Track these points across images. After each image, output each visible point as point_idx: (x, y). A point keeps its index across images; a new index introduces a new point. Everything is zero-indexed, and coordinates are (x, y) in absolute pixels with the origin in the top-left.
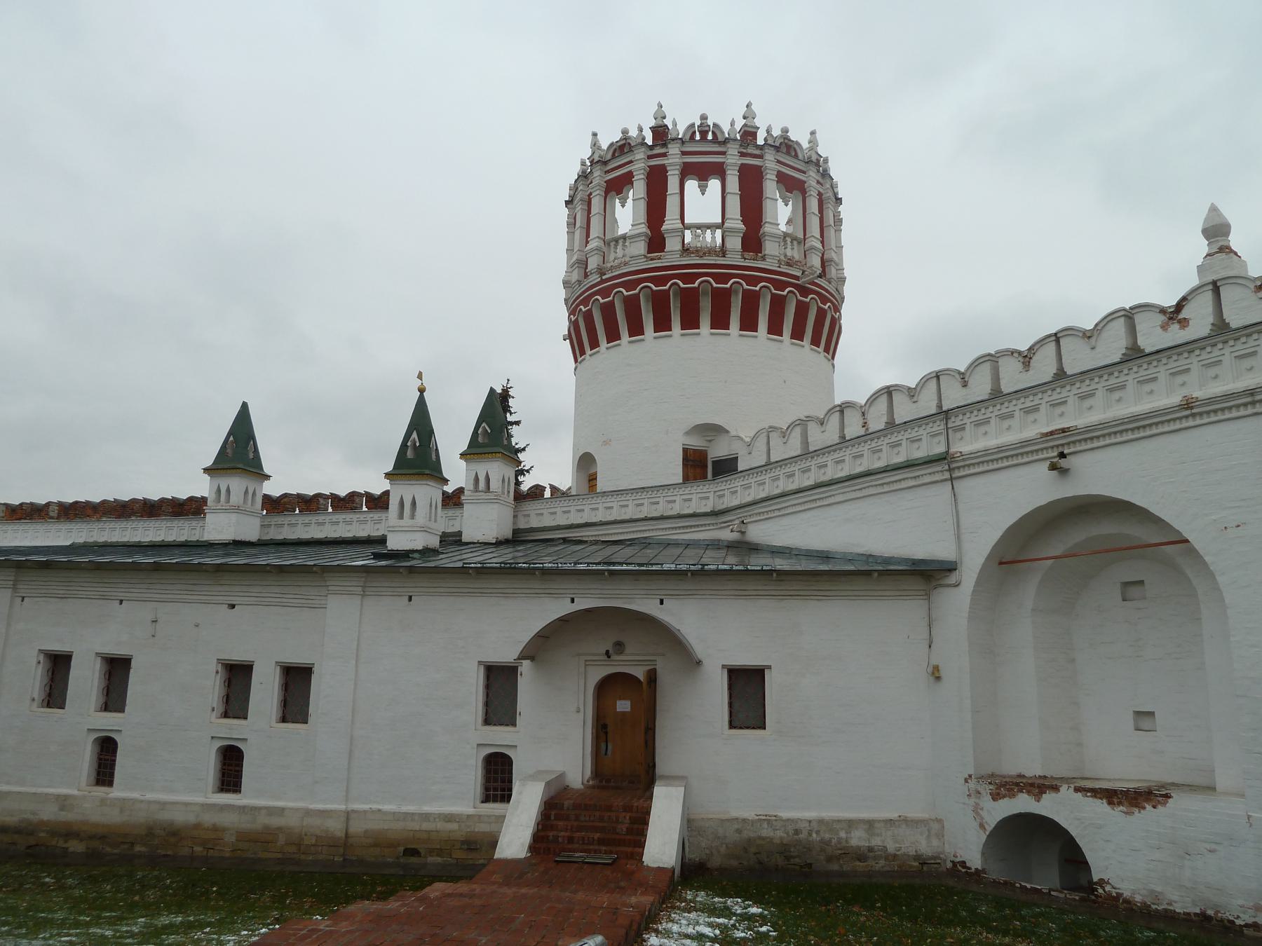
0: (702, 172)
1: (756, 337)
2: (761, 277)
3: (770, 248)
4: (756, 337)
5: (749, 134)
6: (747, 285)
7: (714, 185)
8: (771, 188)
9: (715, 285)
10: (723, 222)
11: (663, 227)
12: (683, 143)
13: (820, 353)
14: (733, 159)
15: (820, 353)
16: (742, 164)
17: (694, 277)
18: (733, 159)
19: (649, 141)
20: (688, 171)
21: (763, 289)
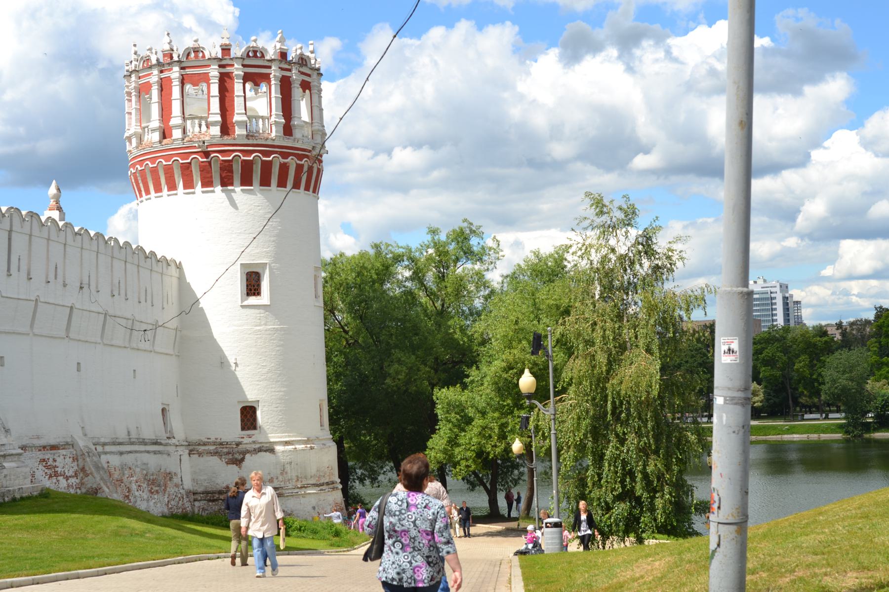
0: (255, 78)
1: (270, 190)
2: (289, 152)
3: (297, 134)
4: (270, 190)
5: (283, 55)
6: (222, 157)
7: (264, 87)
8: (297, 91)
9: (201, 160)
10: (271, 116)
11: (172, 120)
12: (244, 59)
13: (310, 195)
14: (275, 72)
15: (310, 195)
16: (283, 76)
17: (251, 152)
18: (275, 72)
19: (220, 56)
20: (247, 78)
21: (256, 157)
